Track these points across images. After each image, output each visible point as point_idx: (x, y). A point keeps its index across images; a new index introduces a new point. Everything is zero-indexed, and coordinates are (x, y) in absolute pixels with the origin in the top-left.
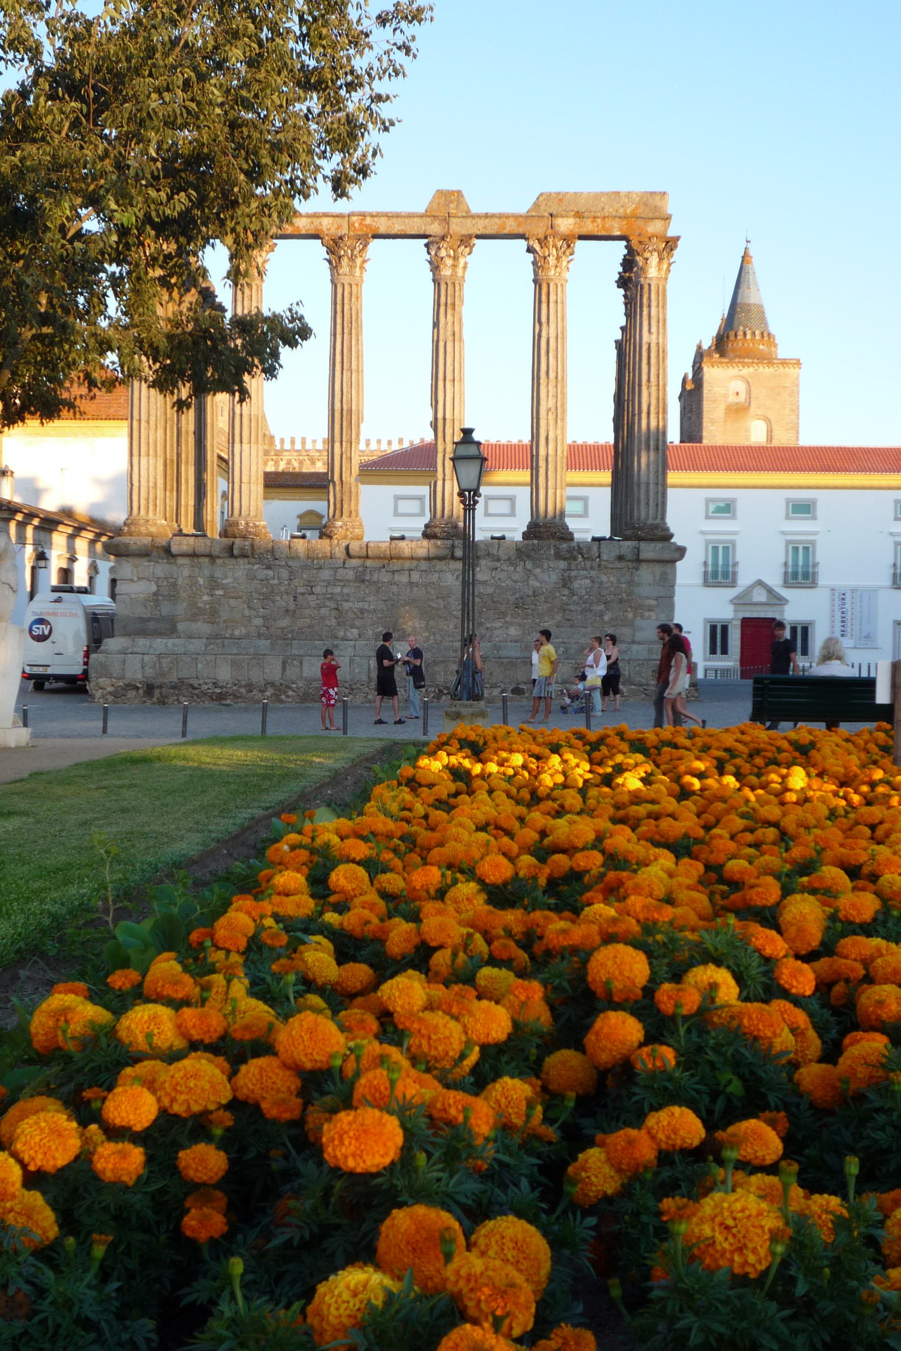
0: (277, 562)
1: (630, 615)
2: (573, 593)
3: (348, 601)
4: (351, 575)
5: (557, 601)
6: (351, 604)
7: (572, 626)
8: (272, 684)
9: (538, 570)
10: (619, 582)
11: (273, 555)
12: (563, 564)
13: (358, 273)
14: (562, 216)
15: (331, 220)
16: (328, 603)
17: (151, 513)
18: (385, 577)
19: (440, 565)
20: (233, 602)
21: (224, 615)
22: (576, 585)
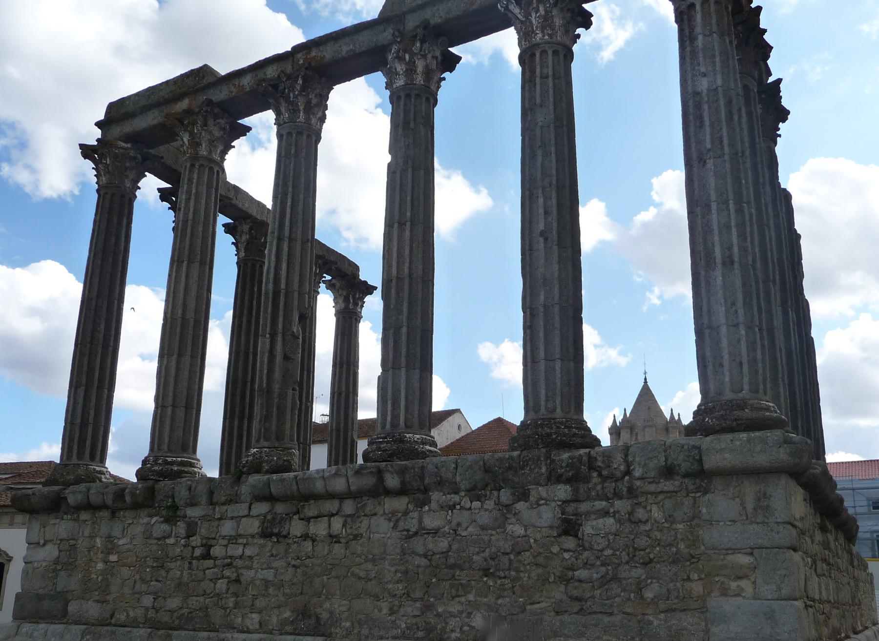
1: (697, 588)
2: (582, 546)
3: (250, 568)
4: (253, 526)
6: (251, 573)
7: (581, 611)
9: (521, 506)
10: (671, 519)
12: (563, 491)
13: (302, 117)
16: (227, 573)
17: (75, 456)
19: (371, 505)
20: (125, 572)
21: (114, 589)
22: (588, 529)
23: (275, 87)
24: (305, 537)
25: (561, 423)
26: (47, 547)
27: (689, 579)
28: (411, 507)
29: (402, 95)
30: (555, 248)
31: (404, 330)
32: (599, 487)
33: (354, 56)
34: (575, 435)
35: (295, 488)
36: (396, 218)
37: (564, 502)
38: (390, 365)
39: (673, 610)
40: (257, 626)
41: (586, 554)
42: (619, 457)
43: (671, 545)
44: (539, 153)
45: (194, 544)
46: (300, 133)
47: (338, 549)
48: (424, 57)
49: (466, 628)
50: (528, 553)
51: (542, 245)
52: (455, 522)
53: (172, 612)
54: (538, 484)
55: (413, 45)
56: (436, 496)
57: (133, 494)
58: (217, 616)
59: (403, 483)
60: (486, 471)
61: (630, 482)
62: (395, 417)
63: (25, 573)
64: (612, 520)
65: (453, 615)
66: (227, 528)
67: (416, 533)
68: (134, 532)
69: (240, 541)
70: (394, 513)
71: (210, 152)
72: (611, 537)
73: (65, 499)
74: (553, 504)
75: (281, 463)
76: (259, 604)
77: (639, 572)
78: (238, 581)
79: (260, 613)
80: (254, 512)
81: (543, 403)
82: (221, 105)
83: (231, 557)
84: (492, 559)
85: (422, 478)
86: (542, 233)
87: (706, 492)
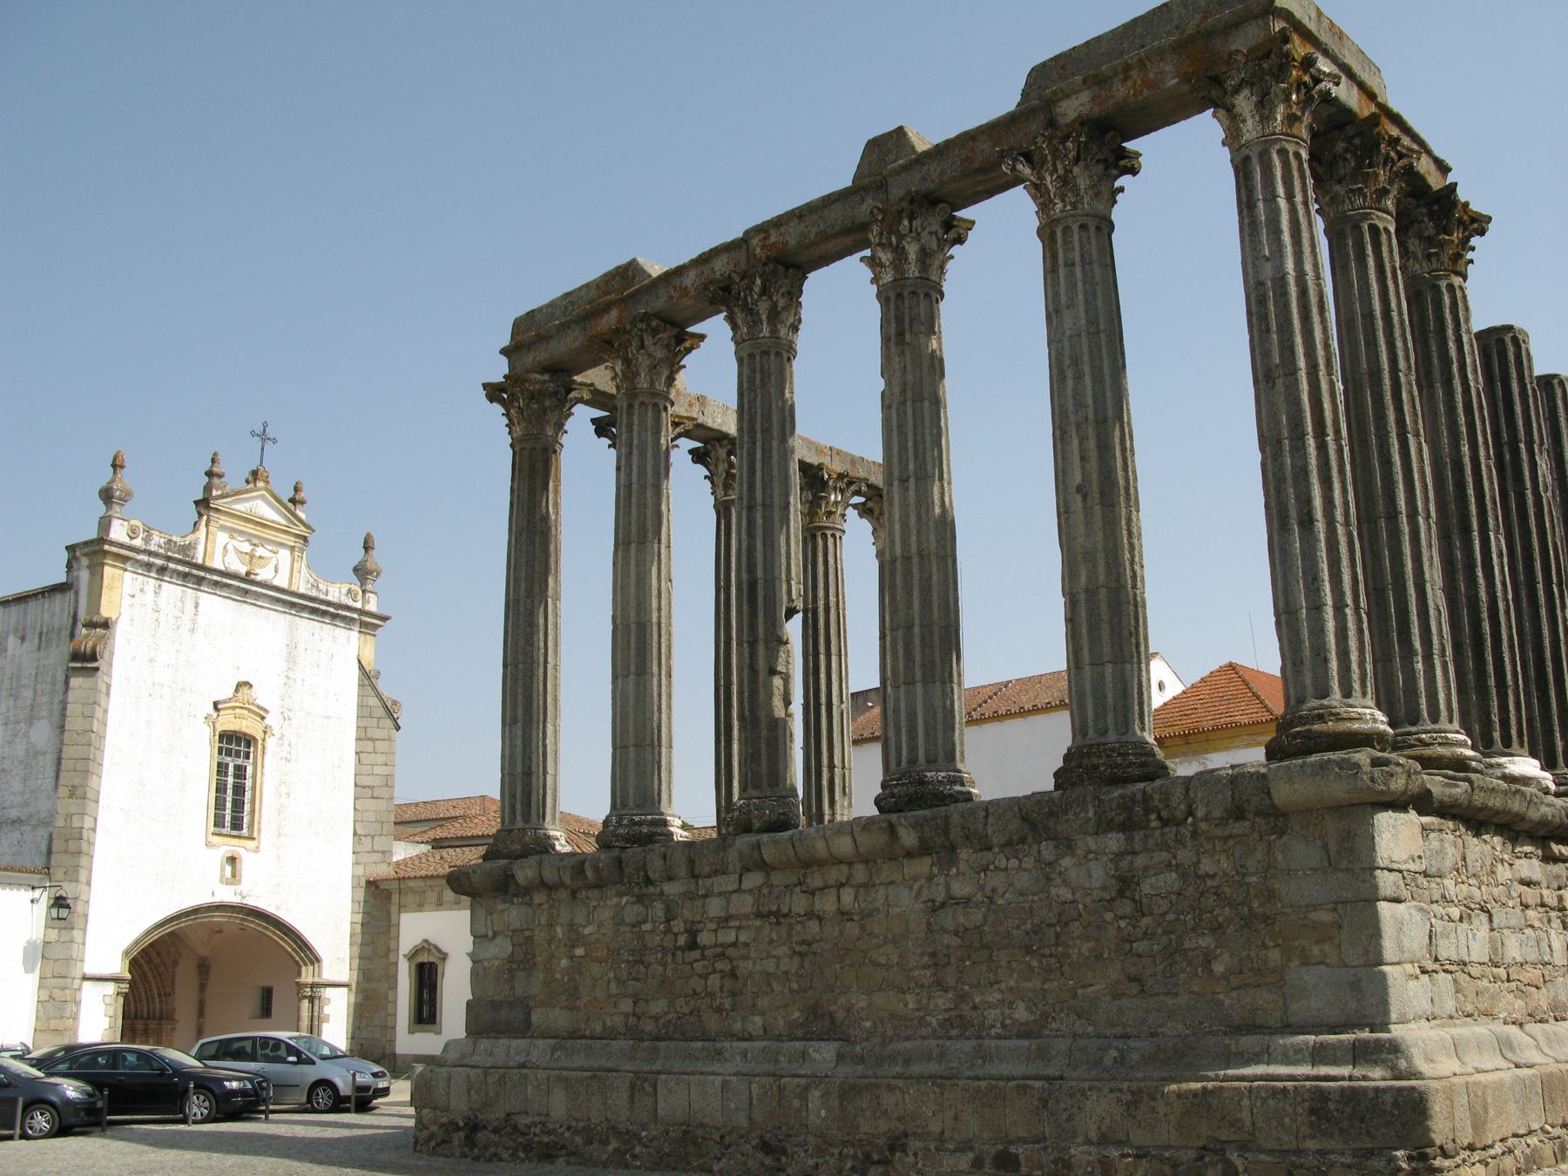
0: (651, 889)
1: (1274, 956)
3: (746, 958)
4: (745, 904)
5: (1112, 931)
8: (618, 1133)
9: (1066, 862)
11: (647, 877)
12: (1114, 841)
13: (765, 331)
14: (1068, 96)
15: (724, 258)
16: (719, 965)
17: (519, 818)
18: (798, 903)
19: (887, 872)
20: (596, 969)
22: (1146, 888)
23: (727, 289)
24: (810, 915)
25: (1113, 750)
26: (497, 941)
27: (1264, 946)
28: (935, 870)
29: (892, 295)
30: (1097, 508)
31: (917, 629)
32: (1158, 832)
33: (824, 237)
34: (1131, 764)
35: (791, 852)
36: (896, 473)
37: (1120, 855)
38: (902, 679)
39: (1247, 985)
40: (761, 1032)
41: (1145, 921)
42: (1179, 792)
43: (1243, 903)
44: (1069, 374)
45: (675, 930)
46: (767, 353)
47: (852, 929)
48: (918, 237)
49: (1008, 1022)
50: (1077, 924)
51: (1080, 505)
52: (988, 889)
53: (656, 1018)
54: (1087, 833)
55: (900, 222)
56: (964, 854)
57: (596, 869)
58: (712, 1022)
59: (922, 840)
60: (1023, 819)
61: (1194, 824)
62: (913, 749)
63: (476, 976)
64: (1174, 875)
65: (990, 1006)
66: (715, 907)
67: (943, 905)
68: (601, 918)
69: (732, 924)
70: (915, 879)
71: (652, 383)
72: (1173, 897)
73: (513, 876)
74: (1105, 859)
75: (774, 818)
76: (763, 1003)
77: (1206, 941)
78: (733, 974)
79: (763, 1014)
80: (746, 885)
81: (1091, 724)
82: (656, 315)
83: (722, 945)
84: (1035, 933)
85: (946, 831)
86: (1079, 489)
87: (1282, 834)
